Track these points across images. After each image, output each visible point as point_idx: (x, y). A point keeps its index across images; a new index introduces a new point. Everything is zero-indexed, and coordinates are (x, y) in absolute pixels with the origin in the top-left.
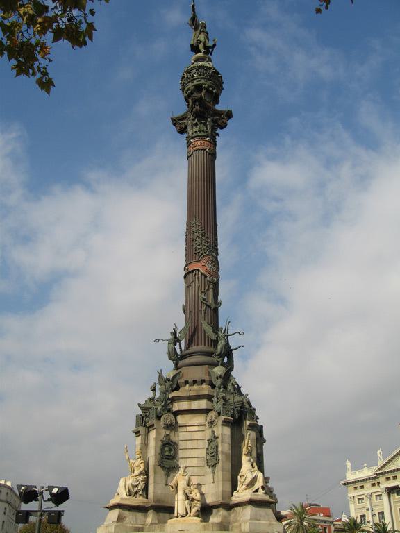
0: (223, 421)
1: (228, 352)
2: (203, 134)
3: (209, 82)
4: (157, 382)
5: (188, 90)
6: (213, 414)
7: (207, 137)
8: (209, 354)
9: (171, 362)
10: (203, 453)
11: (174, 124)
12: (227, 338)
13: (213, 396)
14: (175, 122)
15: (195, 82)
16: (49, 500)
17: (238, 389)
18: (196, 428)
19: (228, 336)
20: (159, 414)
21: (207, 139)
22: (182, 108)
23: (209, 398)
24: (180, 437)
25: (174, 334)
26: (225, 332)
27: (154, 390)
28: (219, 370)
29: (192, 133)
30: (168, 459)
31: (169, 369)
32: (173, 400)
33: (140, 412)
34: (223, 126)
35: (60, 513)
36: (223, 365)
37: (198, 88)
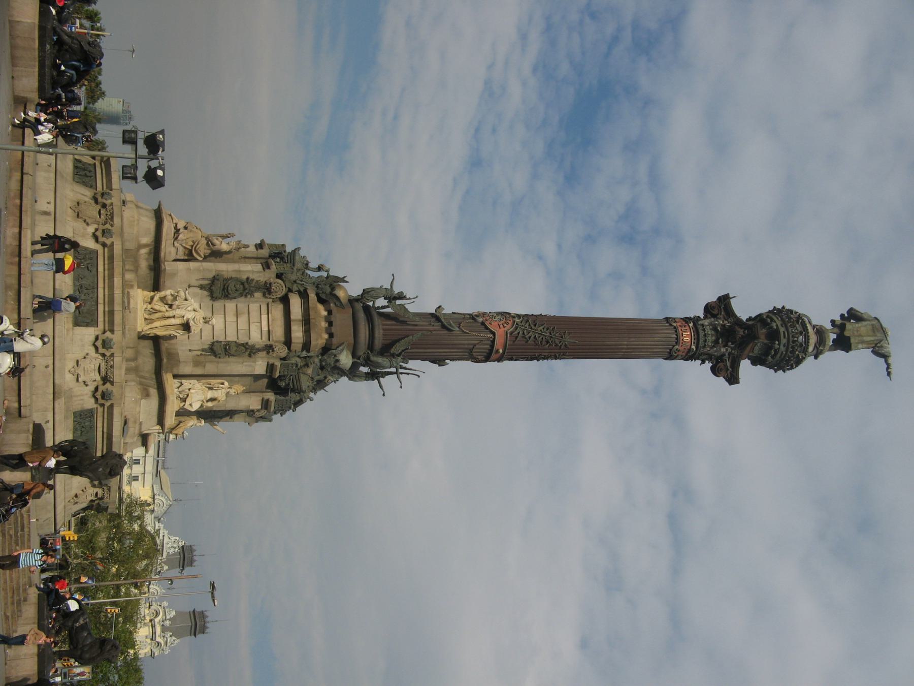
0: (273, 365)
1: (373, 376)
2: (701, 341)
3: (782, 348)
4: (331, 274)
5: (772, 320)
6: (284, 352)
7: (697, 347)
8: (371, 347)
9: (360, 292)
10: (231, 337)
11: (719, 298)
12: (391, 373)
13: (308, 351)
14: (724, 300)
15: (782, 330)
16: (149, 167)
17: (320, 384)
18: (265, 328)
19: (396, 373)
20: (285, 274)
21: (693, 347)
22: (744, 310)
23: (306, 346)
24: (255, 305)
25: (401, 296)
26: (402, 367)
27: (320, 268)
28: (346, 359)
29: (703, 325)
30: (224, 289)
31: (353, 289)
32: (304, 295)
33: (289, 249)
34: (715, 371)
35: (134, 178)
36: (355, 366)
37: (774, 335)
